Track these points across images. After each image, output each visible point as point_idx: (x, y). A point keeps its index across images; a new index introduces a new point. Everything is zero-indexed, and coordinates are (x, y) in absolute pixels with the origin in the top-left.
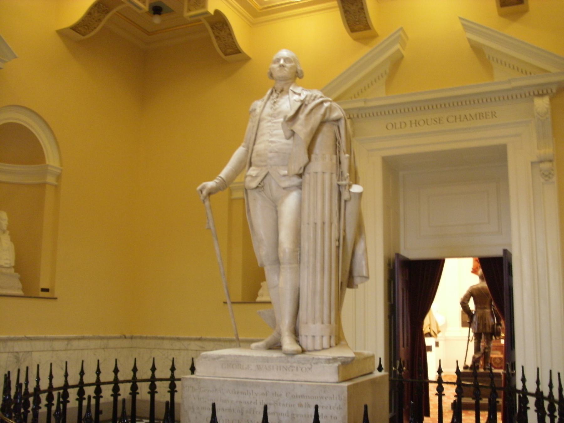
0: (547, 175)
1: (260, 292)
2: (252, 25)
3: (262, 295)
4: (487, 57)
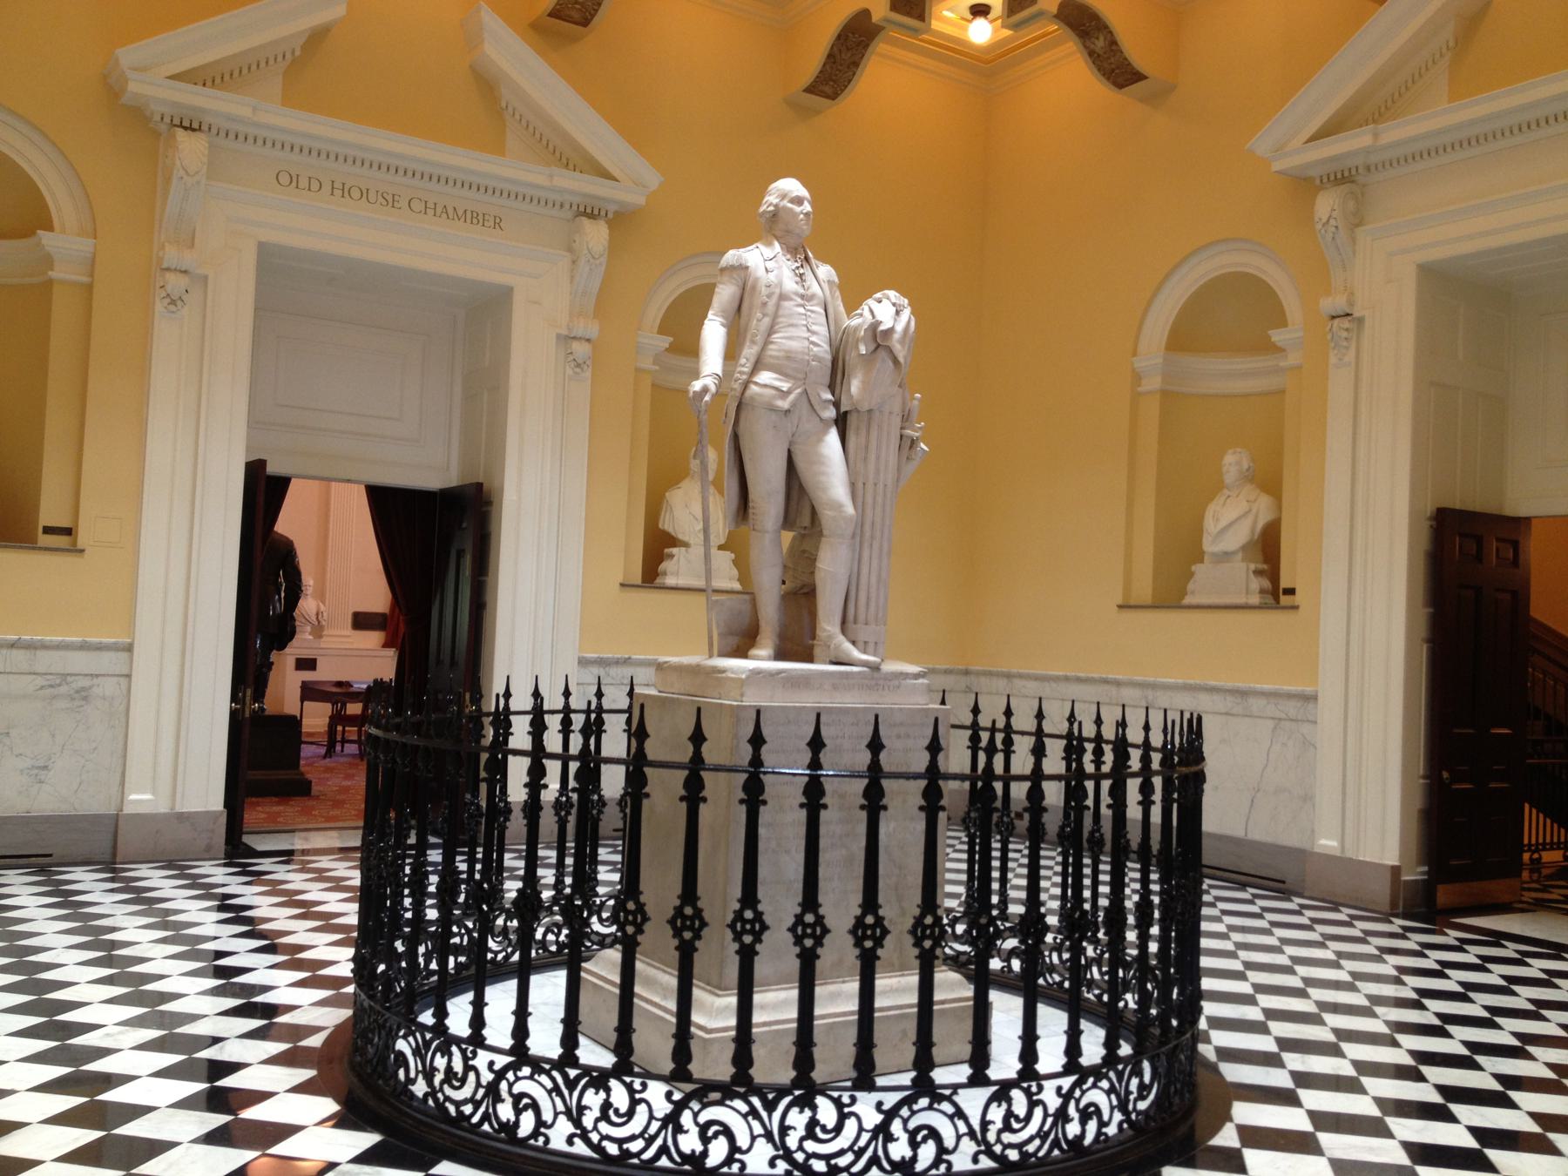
4: (504, 105)
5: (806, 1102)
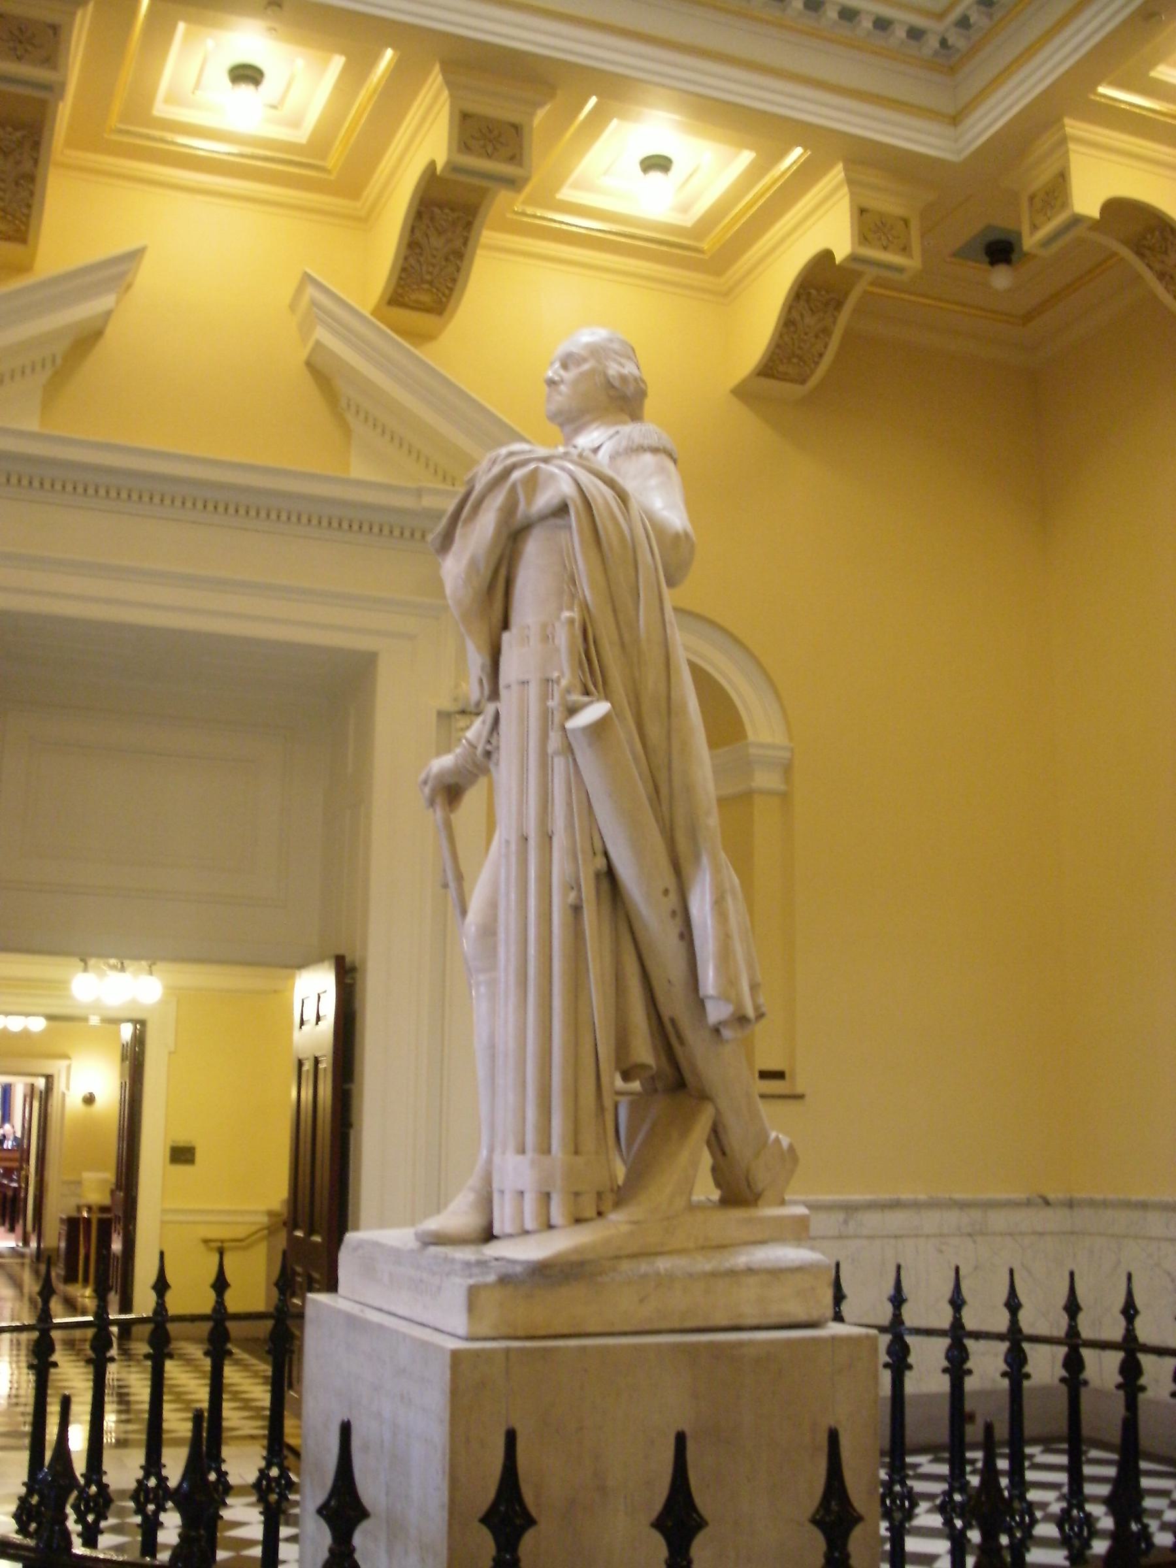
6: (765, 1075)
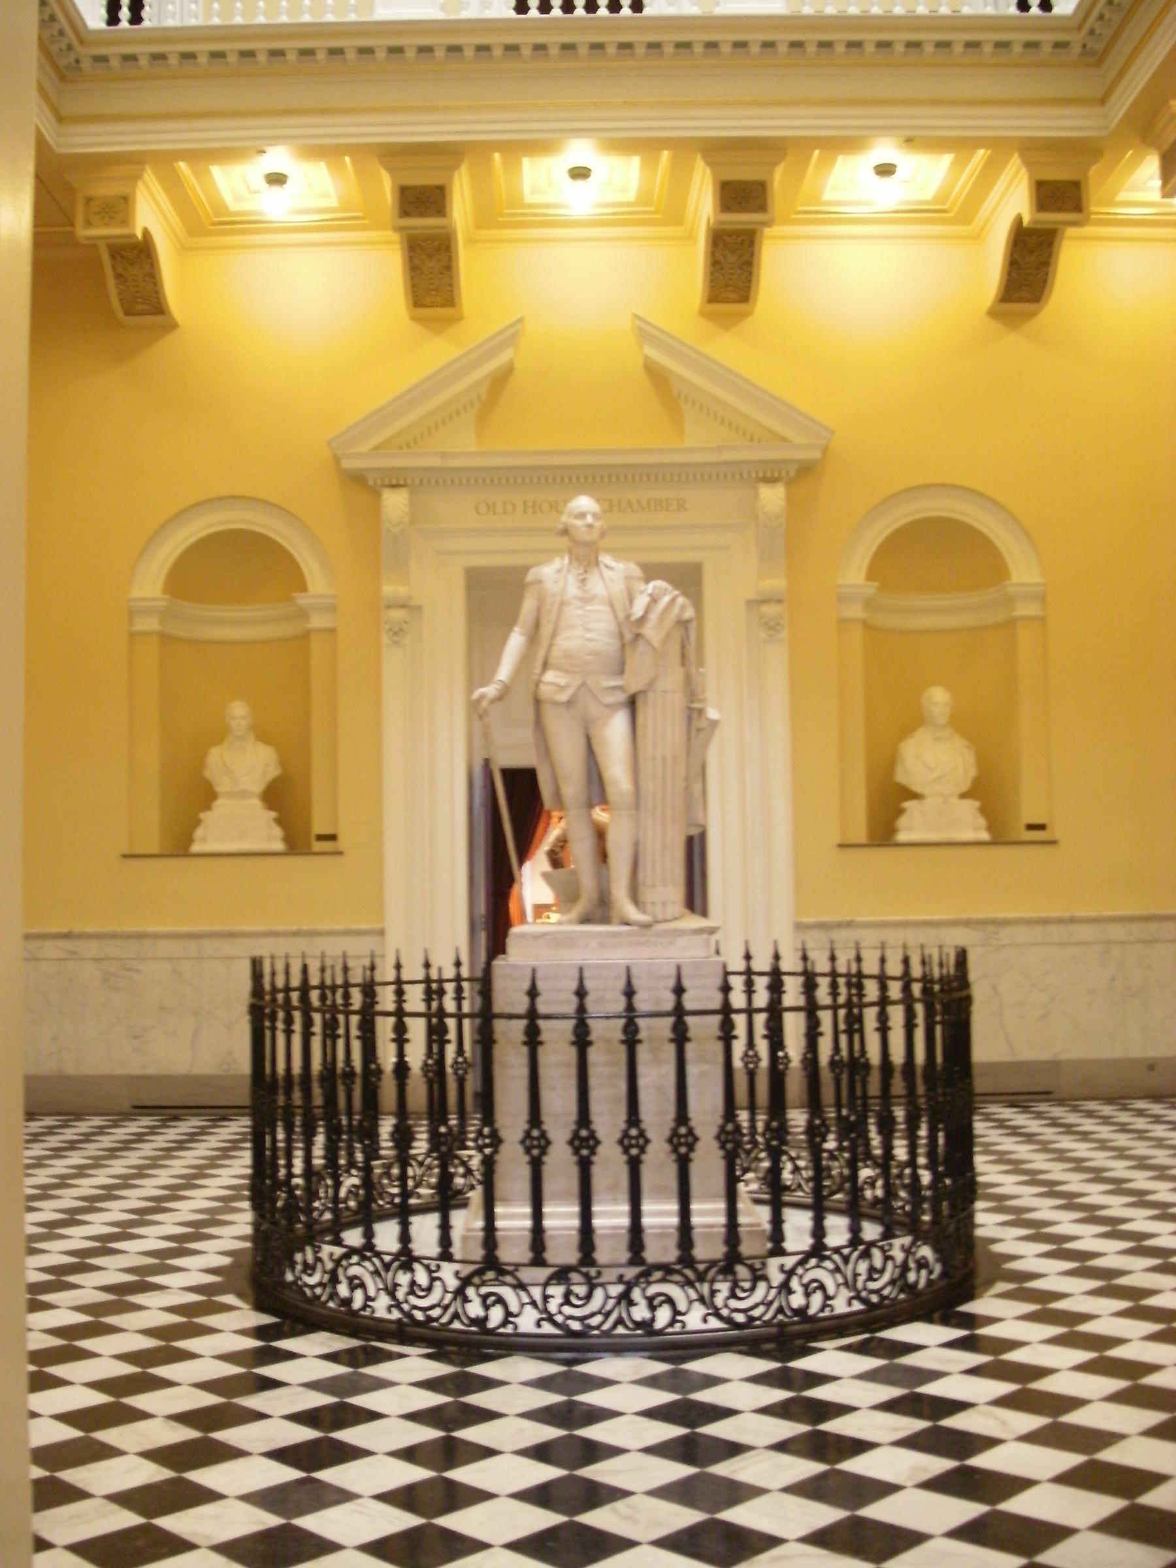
0: (772, 626)
1: (199, 833)
2: (184, 249)
3: (204, 840)
5: (407, 1267)
6: (1031, 827)
